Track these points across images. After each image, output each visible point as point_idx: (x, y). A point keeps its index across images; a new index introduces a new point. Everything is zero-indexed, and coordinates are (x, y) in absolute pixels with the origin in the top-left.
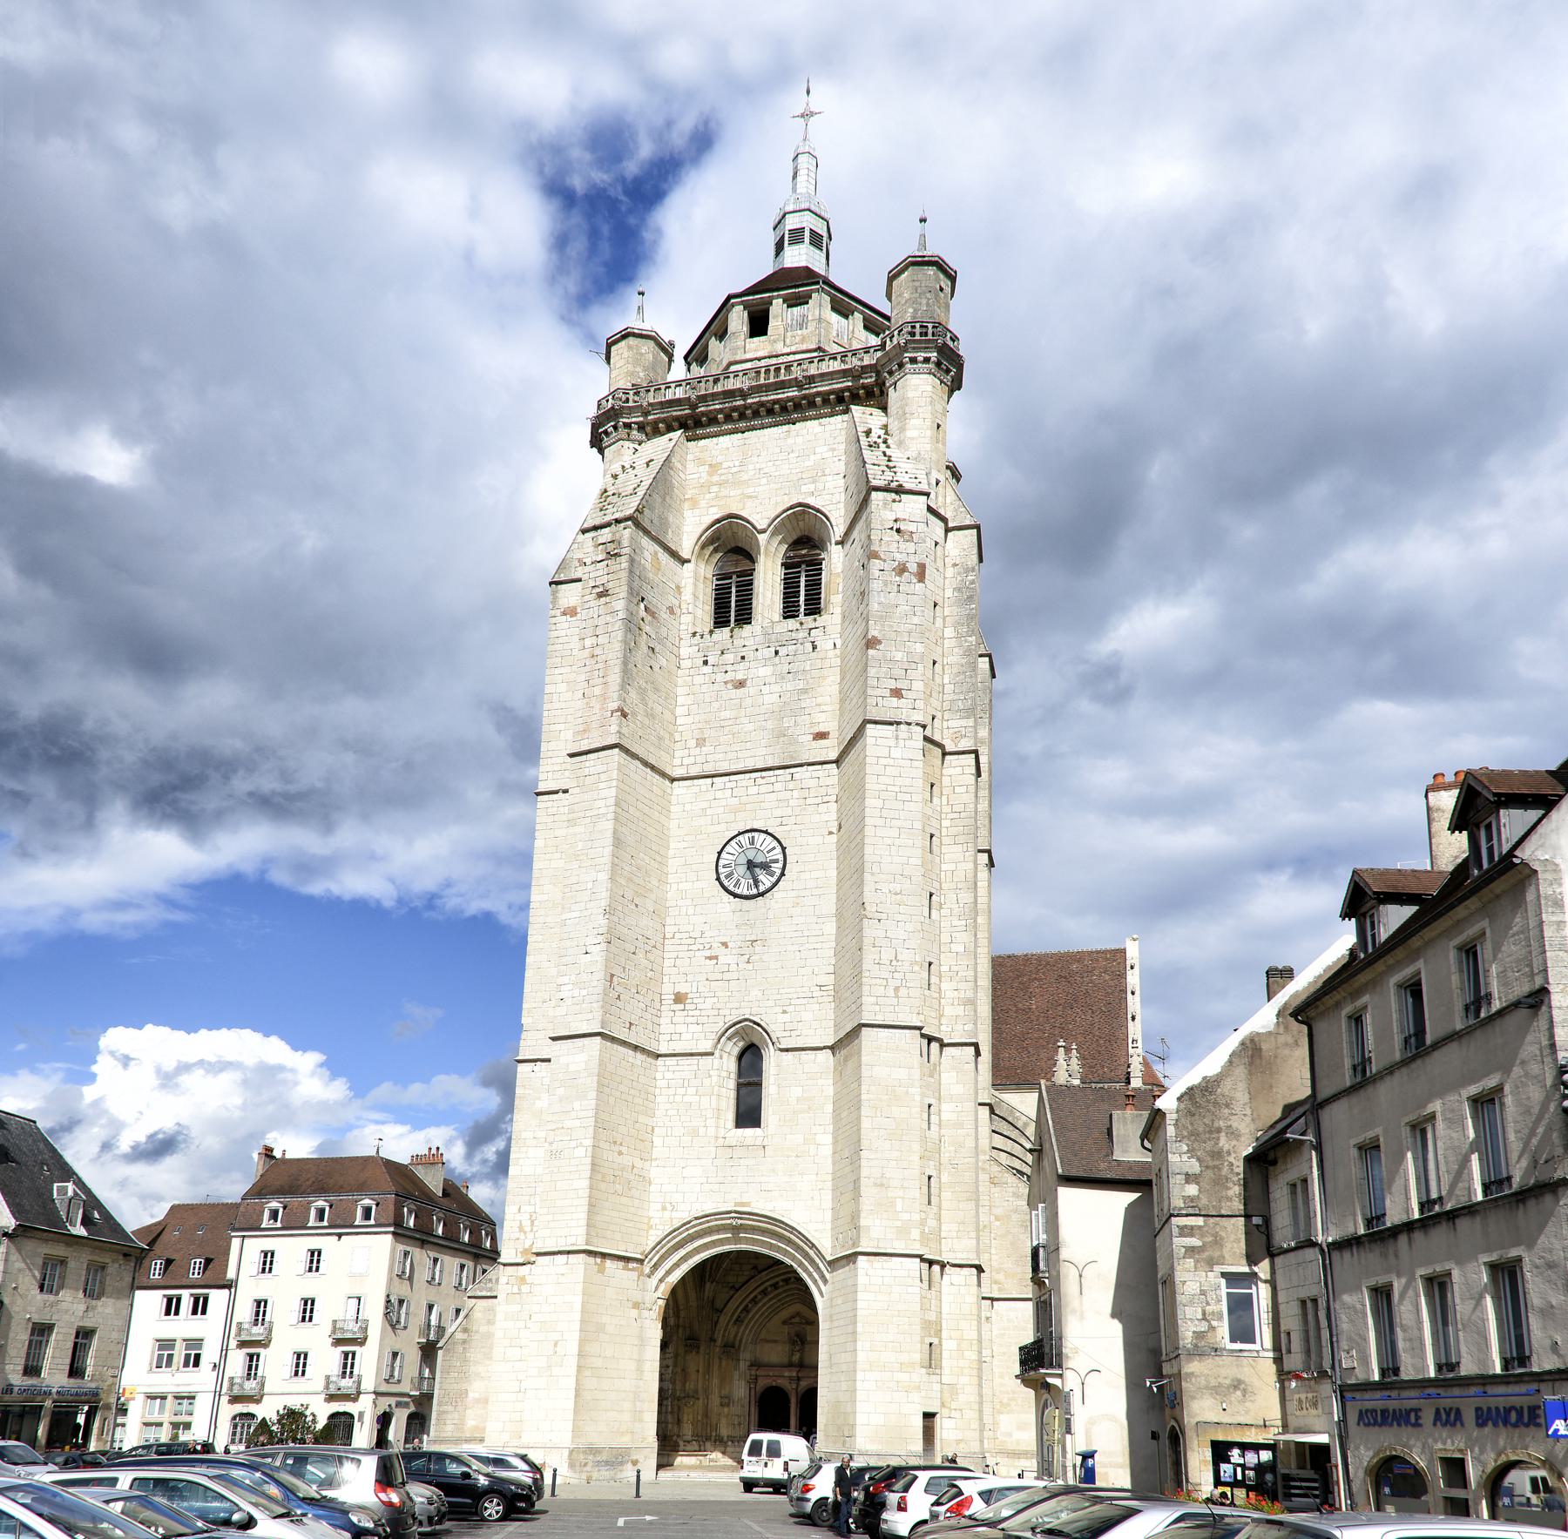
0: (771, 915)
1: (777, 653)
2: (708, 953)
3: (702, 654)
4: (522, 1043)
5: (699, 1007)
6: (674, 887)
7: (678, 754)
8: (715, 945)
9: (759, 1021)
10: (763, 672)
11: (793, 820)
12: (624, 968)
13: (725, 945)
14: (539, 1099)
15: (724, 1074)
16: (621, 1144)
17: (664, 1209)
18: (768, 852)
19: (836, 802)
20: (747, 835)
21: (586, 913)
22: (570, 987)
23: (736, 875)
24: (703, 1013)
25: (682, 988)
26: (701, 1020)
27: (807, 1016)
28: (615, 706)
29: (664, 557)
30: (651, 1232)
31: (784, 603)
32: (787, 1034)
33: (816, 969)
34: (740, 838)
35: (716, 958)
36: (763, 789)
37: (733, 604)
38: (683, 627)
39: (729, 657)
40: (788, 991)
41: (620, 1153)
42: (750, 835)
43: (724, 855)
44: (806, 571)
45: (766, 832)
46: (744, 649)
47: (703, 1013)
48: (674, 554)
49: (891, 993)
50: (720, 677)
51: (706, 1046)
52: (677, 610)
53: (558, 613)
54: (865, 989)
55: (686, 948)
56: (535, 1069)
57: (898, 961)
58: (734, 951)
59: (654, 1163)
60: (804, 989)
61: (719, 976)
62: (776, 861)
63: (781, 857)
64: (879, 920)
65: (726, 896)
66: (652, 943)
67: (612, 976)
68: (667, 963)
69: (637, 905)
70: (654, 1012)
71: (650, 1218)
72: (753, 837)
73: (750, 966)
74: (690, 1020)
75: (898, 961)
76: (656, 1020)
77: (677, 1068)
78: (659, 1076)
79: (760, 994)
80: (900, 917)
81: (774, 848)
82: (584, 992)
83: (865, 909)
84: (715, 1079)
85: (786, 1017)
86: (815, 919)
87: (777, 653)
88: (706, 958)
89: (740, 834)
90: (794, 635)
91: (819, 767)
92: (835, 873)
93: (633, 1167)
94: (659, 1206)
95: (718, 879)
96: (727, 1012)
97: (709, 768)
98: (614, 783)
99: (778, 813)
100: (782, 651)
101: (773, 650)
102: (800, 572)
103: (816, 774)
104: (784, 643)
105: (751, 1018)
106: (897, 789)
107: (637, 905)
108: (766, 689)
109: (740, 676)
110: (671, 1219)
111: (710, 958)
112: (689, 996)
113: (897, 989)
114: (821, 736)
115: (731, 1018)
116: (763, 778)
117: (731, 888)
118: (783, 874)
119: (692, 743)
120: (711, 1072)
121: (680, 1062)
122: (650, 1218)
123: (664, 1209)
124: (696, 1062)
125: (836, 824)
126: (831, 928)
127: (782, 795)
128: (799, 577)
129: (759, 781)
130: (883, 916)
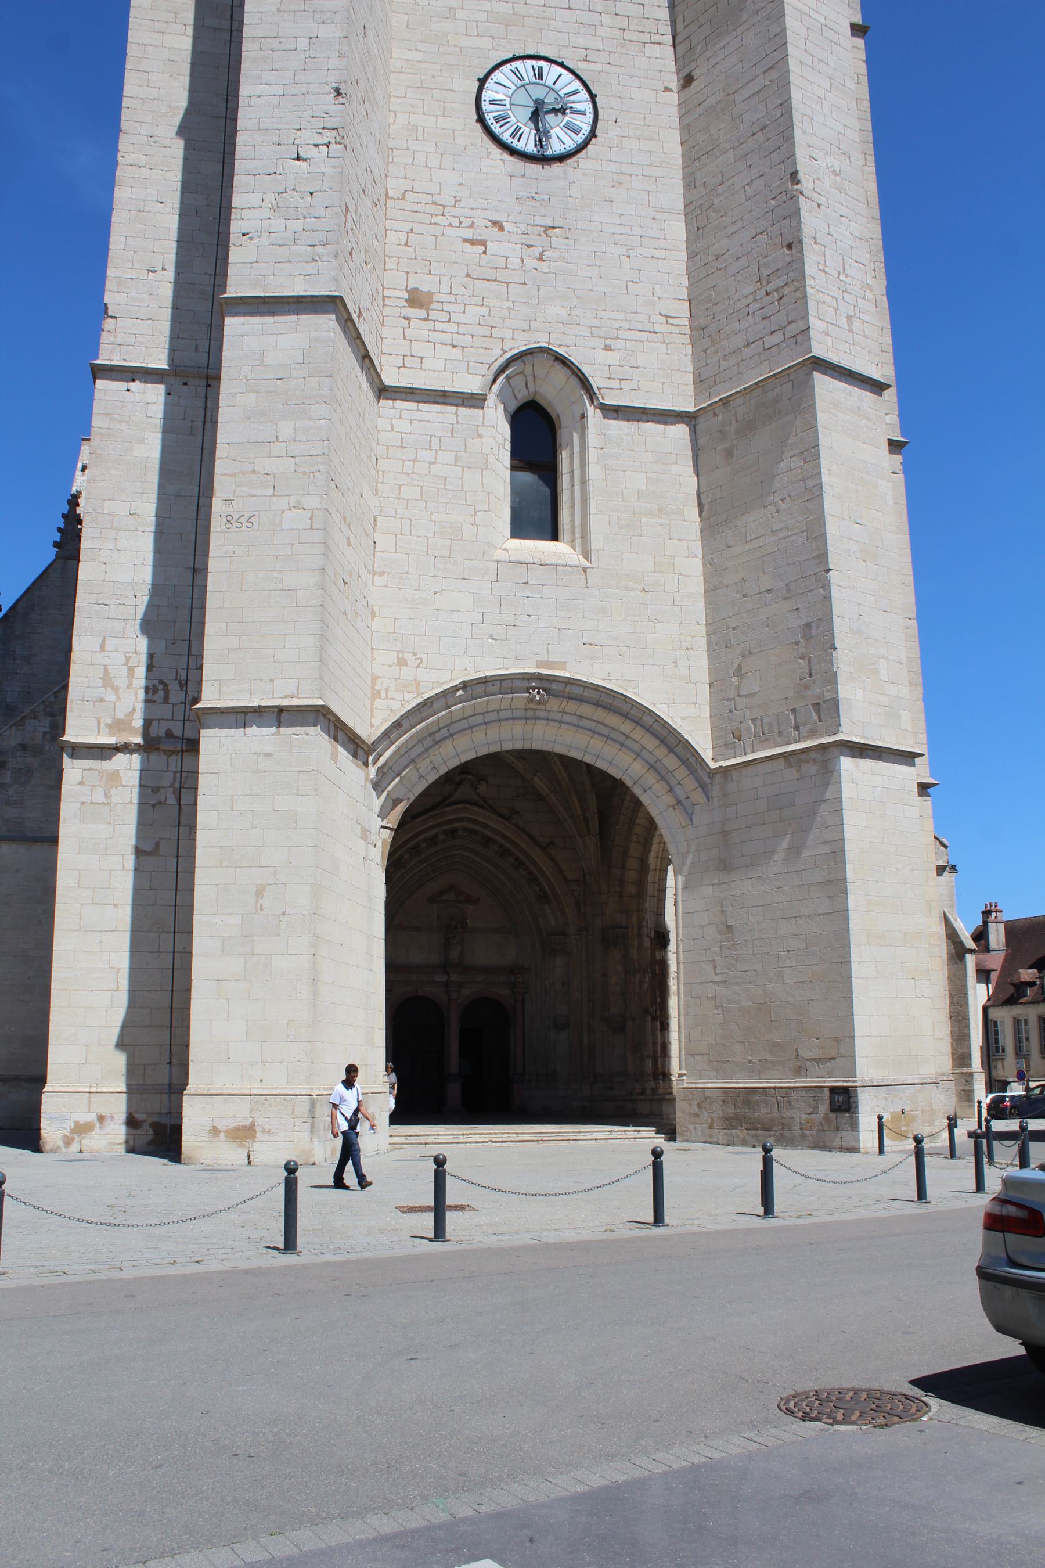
0: (575, 192)
2: (469, 234)
4: (105, 337)
6: (402, 119)
8: (480, 222)
11: (604, 57)
13: (497, 225)
15: (500, 440)
17: (402, 662)
20: (530, 63)
21: (295, 90)
22: (266, 213)
24: (462, 329)
25: (424, 284)
26: (458, 339)
30: (378, 702)
32: (616, 384)
33: (657, 287)
34: (518, 64)
35: (483, 243)
42: (534, 63)
43: (490, 83)
45: (561, 65)
47: (462, 329)
49: (843, 322)
51: (472, 385)
54: (811, 304)
55: (427, 219)
57: (847, 276)
58: (514, 238)
61: (491, 274)
62: (583, 113)
63: (588, 107)
64: (819, 206)
65: (496, 152)
68: (392, 238)
71: (375, 678)
72: (541, 69)
73: (544, 266)
77: (418, 415)
79: (564, 313)
80: (844, 211)
81: (575, 92)
82: (297, 225)
83: (798, 182)
85: (612, 358)
88: (465, 240)
89: (515, 58)
92: (678, 150)
94: (392, 657)
95: (481, 120)
96: (508, 335)
99: (581, 42)
110: (418, 684)
111: (472, 242)
112: (435, 298)
113: (849, 318)
115: (514, 344)
117: (506, 137)
118: (593, 134)
120: (482, 430)
122: (375, 678)
123: (402, 662)
125: (675, 77)
126: (678, 229)
130: (823, 201)
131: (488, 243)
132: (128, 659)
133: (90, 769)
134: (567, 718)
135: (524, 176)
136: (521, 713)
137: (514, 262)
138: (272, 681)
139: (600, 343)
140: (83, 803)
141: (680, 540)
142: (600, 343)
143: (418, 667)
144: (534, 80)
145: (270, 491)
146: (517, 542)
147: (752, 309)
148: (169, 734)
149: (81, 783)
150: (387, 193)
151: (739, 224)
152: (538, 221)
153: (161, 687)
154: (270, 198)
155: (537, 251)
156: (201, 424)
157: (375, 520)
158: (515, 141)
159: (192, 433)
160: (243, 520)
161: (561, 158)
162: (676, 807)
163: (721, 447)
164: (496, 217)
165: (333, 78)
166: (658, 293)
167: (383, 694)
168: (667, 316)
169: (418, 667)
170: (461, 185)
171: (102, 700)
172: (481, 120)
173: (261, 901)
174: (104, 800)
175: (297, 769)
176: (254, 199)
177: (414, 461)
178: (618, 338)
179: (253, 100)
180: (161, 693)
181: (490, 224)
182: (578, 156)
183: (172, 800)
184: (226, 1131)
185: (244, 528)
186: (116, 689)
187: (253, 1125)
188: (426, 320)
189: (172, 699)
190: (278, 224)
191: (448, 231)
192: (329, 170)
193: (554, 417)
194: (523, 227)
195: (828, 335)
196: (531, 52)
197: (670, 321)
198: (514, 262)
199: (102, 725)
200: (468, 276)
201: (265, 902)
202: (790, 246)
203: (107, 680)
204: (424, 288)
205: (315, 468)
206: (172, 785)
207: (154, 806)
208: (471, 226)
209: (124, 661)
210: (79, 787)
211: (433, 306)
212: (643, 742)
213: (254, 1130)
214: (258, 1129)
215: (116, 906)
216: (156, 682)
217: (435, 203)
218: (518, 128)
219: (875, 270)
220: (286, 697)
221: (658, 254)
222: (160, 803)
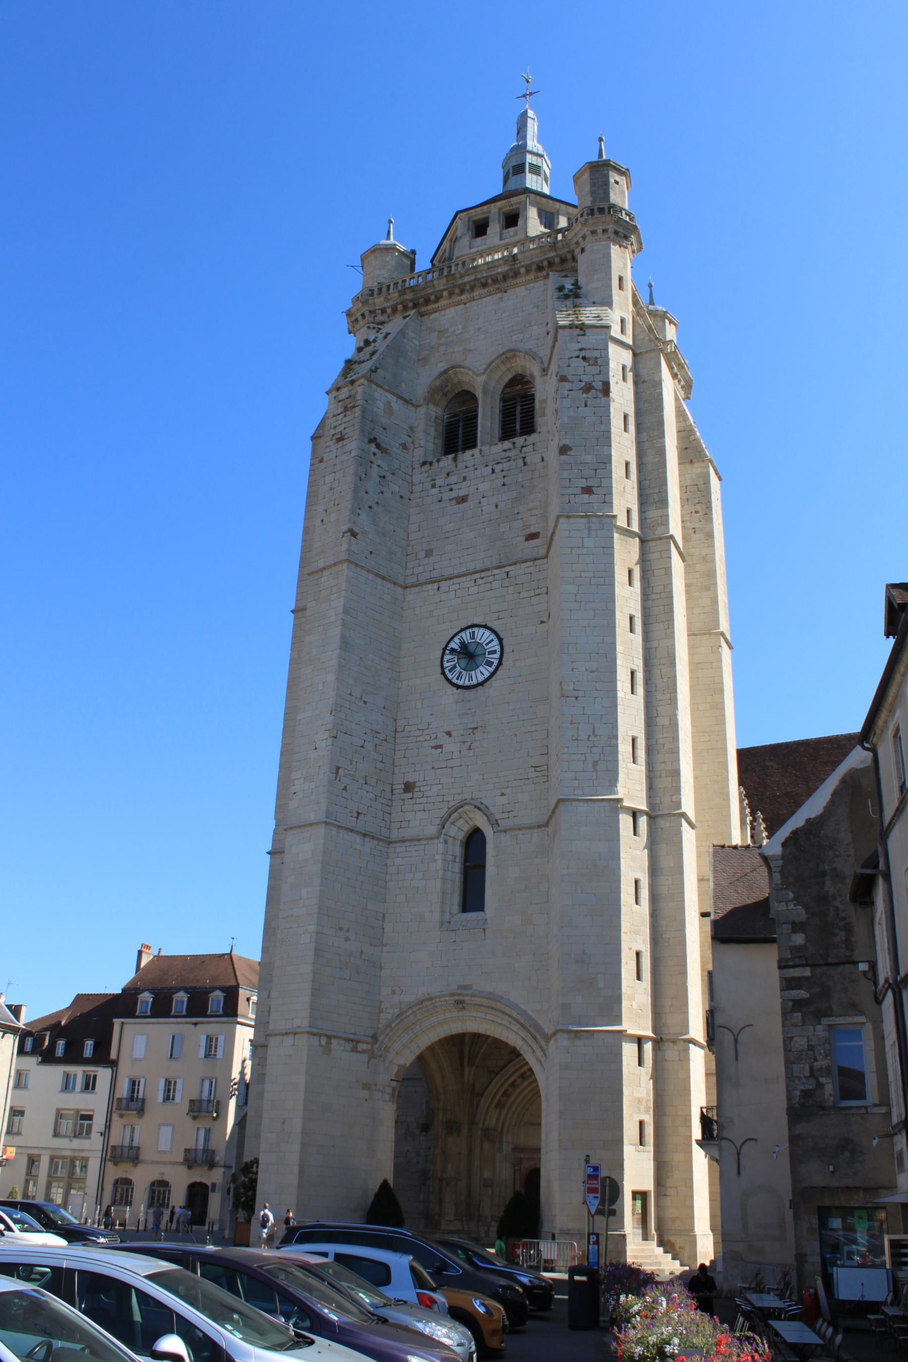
1: (493, 471)
2: (433, 743)
3: (430, 479)
5: (426, 794)
7: (410, 565)
9: (478, 805)
10: (482, 487)
12: (351, 761)
13: (449, 734)
15: (450, 858)
16: (348, 930)
17: (394, 993)
18: (487, 644)
20: (468, 632)
22: (302, 781)
23: (458, 668)
28: (345, 528)
29: (396, 404)
30: (382, 1016)
31: (503, 429)
32: (505, 815)
35: (441, 746)
36: (482, 588)
37: (460, 436)
38: (415, 459)
39: (453, 479)
41: (347, 939)
42: (471, 630)
44: (521, 402)
45: (485, 627)
46: (467, 470)
48: (407, 402)
50: (447, 496)
52: (411, 446)
57: (596, 736)
59: (385, 949)
62: (494, 652)
63: (498, 648)
64: (577, 698)
66: (382, 736)
67: (338, 768)
69: (365, 702)
70: (385, 801)
72: (474, 632)
73: (471, 753)
74: (417, 807)
75: (596, 736)
76: (387, 809)
78: (390, 862)
81: (492, 640)
84: (439, 864)
85: (504, 800)
87: (493, 471)
89: (462, 630)
90: (508, 454)
91: (531, 563)
93: (362, 953)
95: (443, 673)
96: (451, 798)
97: (436, 574)
98: (343, 594)
100: (498, 468)
101: (490, 468)
102: (515, 403)
103: (528, 571)
104: (499, 461)
105: (472, 802)
106: (591, 575)
107: (365, 702)
108: (484, 501)
109: (462, 493)
110: (400, 1003)
111: (436, 747)
112: (417, 785)
113: (595, 764)
114: (532, 536)
117: (454, 681)
118: (500, 664)
119: (422, 554)
120: (437, 857)
121: (408, 849)
122: (381, 1002)
124: (422, 847)
128: (515, 407)
129: (480, 581)
130: (581, 694)
135: (463, 700)
141: (537, 904)
143: (401, 994)
144: (470, 641)
146: (465, 915)
150: (396, 729)
152: (470, 726)
155: (469, 743)
157: (384, 916)
158: (459, 681)
161: (481, 684)
164: (447, 729)
167: (384, 1011)
168: (535, 767)
169: (401, 994)
170: (432, 715)
172: (443, 673)
177: (404, 880)
178: (508, 787)
181: (445, 734)
182: (492, 679)
188: (412, 798)
191: (425, 744)
194: (461, 732)
195: (576, 779)
196: (469, 624)
197: (537, 769)
200: (433, 768)
204: (411, 781)
208: (436, 738)
211: (417, 789)
217: (419, 729)
218: (461, 672)
219: (670, 699)
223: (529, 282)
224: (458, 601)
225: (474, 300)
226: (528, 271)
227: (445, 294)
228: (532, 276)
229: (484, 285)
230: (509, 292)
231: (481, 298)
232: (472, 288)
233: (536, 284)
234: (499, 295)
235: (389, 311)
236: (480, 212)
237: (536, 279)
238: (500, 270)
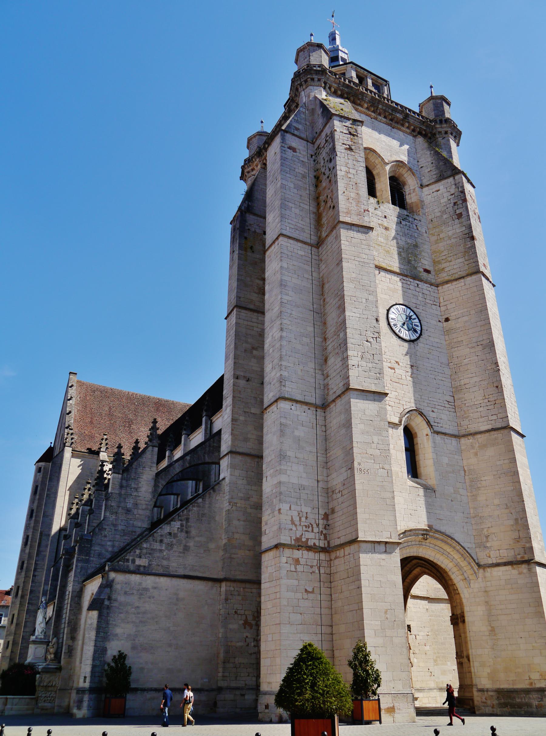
2: (389, 365)
11: (421, 307)
14: (297, 429)
19: (440, 306)
21: (364, 316)
27: (444, 417)
32: (436, 424)
34: (397, 306)
35: (394, 369)
39: (378, 212)
40: (434, 400)
43: (390, 312)
45: (410, 308)
46: (385, 213)
53: (286, 146)
56: (293, 407)
60: (440, 401)
61: (397, 380)
62: (417, 326)
63: (419, 324)
65: (394, 337)
79: (419, 397)
86: (439, 364)
88: (389, 367)
91: (429, 286)
95: (389, 324)
111: (391, 368)
116: (404, 280)
117: (397, 331)
118: (421, 334)
127: (414, 292)
131: (396, 369)
132: (299, 514)
133: (289, 557)
134: (431, 545)
136: (417, 543)
137: (404, 377)
138: (382, 532)
139: (430, 409)
140: (288, 571)
142: (430, 409)
145: (373, 461)
147: (482, 405)
148: (314, 544)
149: (286, 563)
151: (474, 375)
153: (310, 526)
154: (360, 354)
156: (315, 425)
159: (313, 428)
160: (365, 471)
162: (464, 580)
163: (472, 451)
165: (375, 314)
166: (445, 393)
171: (291, 530)
172: (389, 324)
173: (387, 616)
174: (295, 570)
175: (394, 566)
176: (355, 353)
178: (435, 408)
179: (350, 317)
180: (311, 528)
181: (395, 362)
183: (317, 571)
184: (384, 709)
185: (366, 474)
186: (296, 525)
187: (394, 706)
189: (314, 531)
190: (364, 364)
192: (378, 347)
193: (413, 433)
197: (449, 403)
198: (404, 377)
199: (292, 540)
200: (391, 380)
201: (388, 616)
202: (497, 387)
203: (293, 522)
205: (386, 455)
206: (317, 565)
207: (311, 573)
209: (298, 515)
210: (286, 564)
212: (454, 555)
213: (394, 709)
214: (395, 708)
215: (301, 614)
216: (309, 524)
220: (387, 538)
221: (443, 379)
222: (313, 572)
223: (406, 132)
224: (391, 286)
225: (376, 120)
226: (408, 128)
227: (366, 105)
228: (408, 131)
229: (385, 117)
230: (395, 130)
231: (380, 121)
232: (380, 114)
233: (408, 136)
234: (390, 127)
235: (333, 90)
236: (362, 72)
237: (410, 134)
238: (398, 115)
